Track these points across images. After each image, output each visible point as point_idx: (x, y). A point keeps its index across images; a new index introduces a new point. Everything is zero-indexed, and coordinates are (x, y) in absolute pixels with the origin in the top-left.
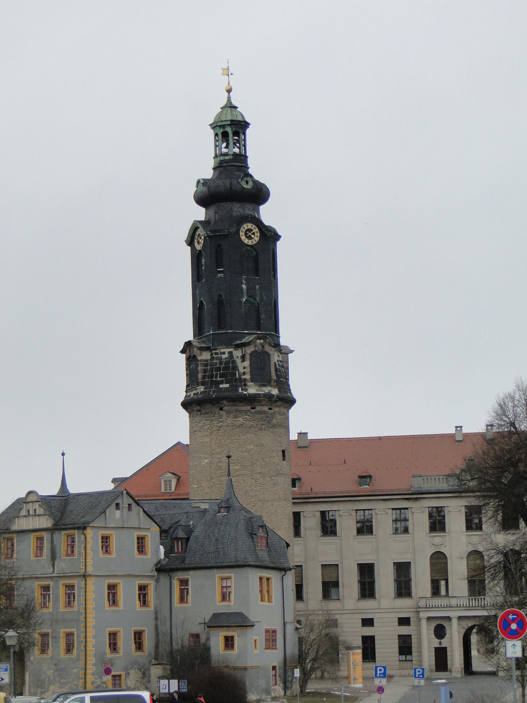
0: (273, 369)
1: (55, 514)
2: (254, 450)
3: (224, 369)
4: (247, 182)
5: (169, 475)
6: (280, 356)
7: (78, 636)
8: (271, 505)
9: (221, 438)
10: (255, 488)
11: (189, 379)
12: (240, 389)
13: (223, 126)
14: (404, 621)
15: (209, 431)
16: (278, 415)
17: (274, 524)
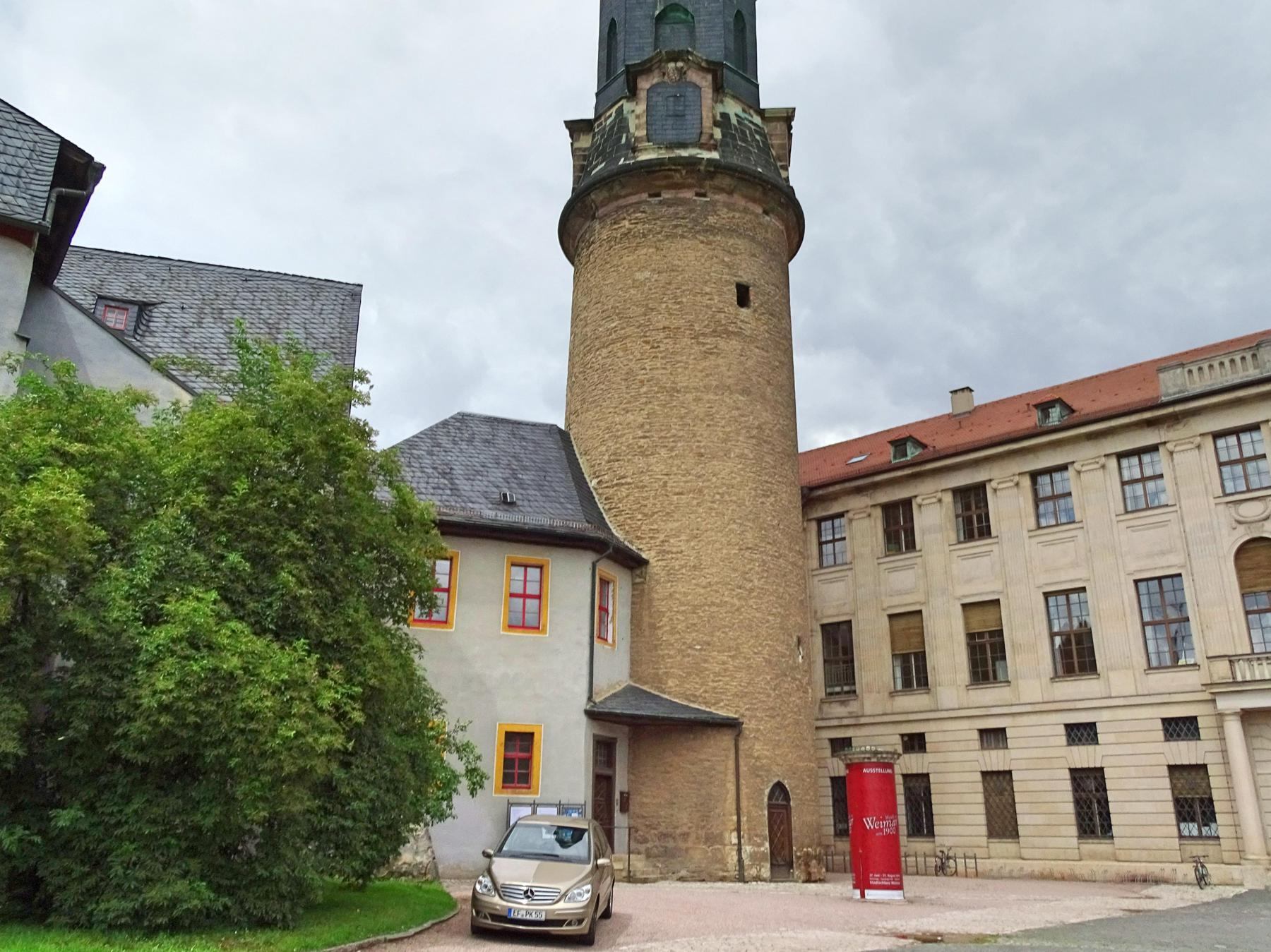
8: (694, 400)
14: (1182, 728)
16: (725, 210)
17: (702, 444)
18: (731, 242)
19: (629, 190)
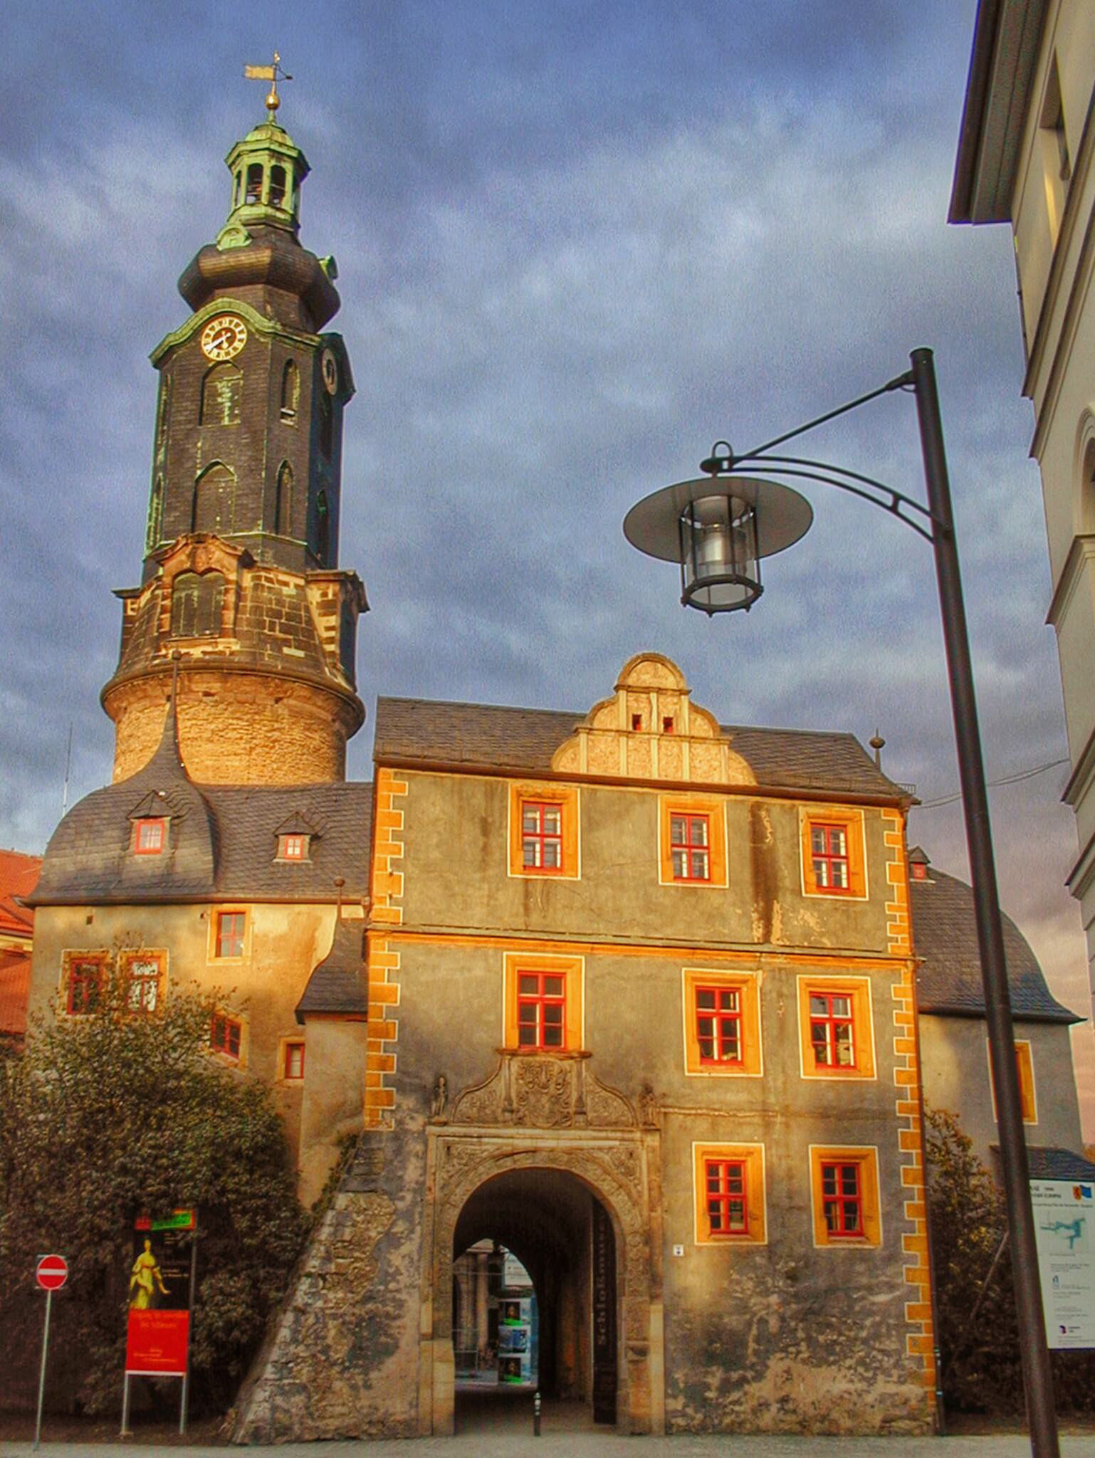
3: (289, 617)
7: (890, 1173)
15: (243, 746)
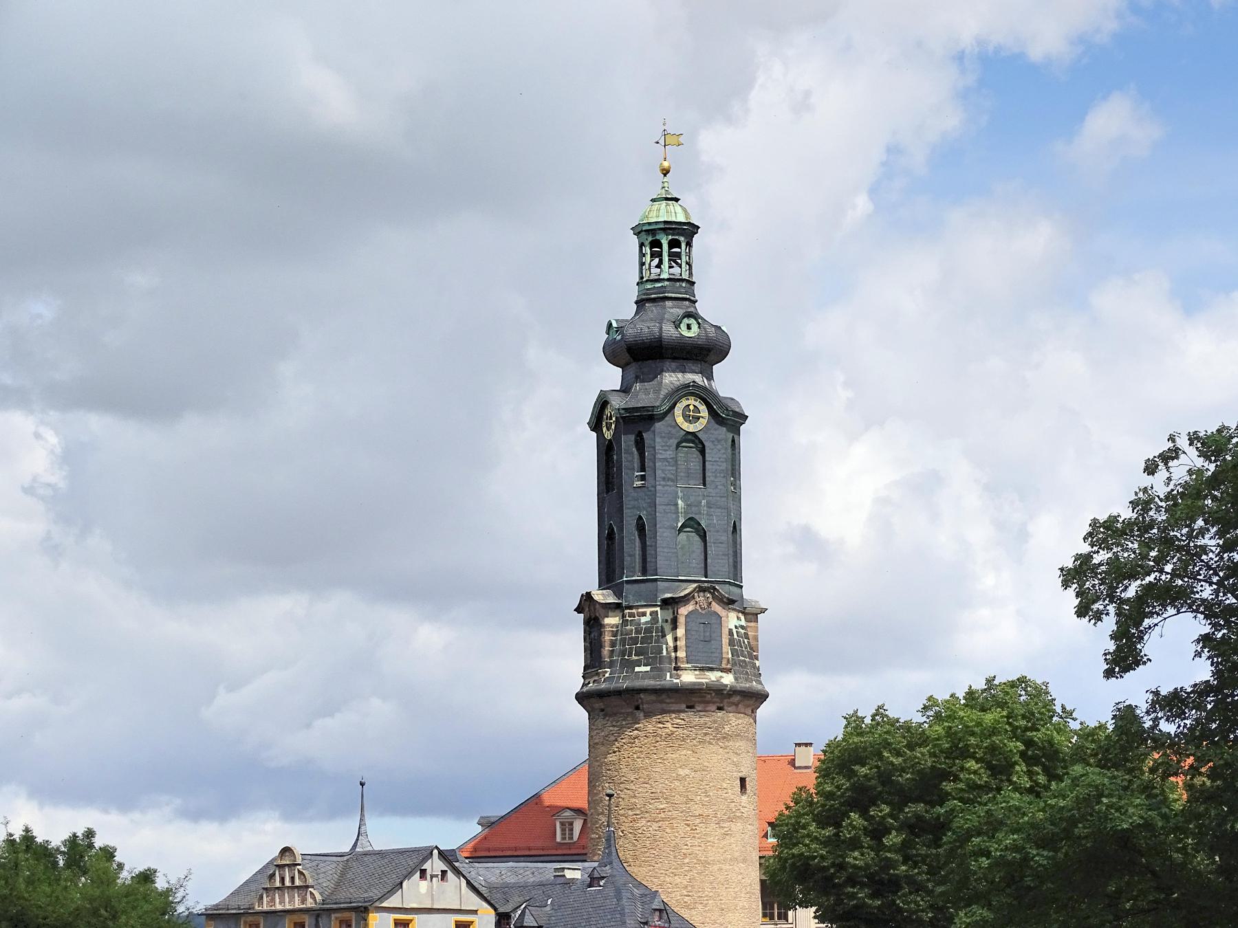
0: (725, 640)
1: (325, 885)
2: (691, 777)
3: (644, 640)
4: (689, 327)
5: (568, 813)
6: (742, 618)
9: (635, 756)
10: (691, 841)
11: (589, 656)
12: (668, 674)
13: (652, 232)
16: (734, 719)
18: (738, 744)
19: (673, 700)
